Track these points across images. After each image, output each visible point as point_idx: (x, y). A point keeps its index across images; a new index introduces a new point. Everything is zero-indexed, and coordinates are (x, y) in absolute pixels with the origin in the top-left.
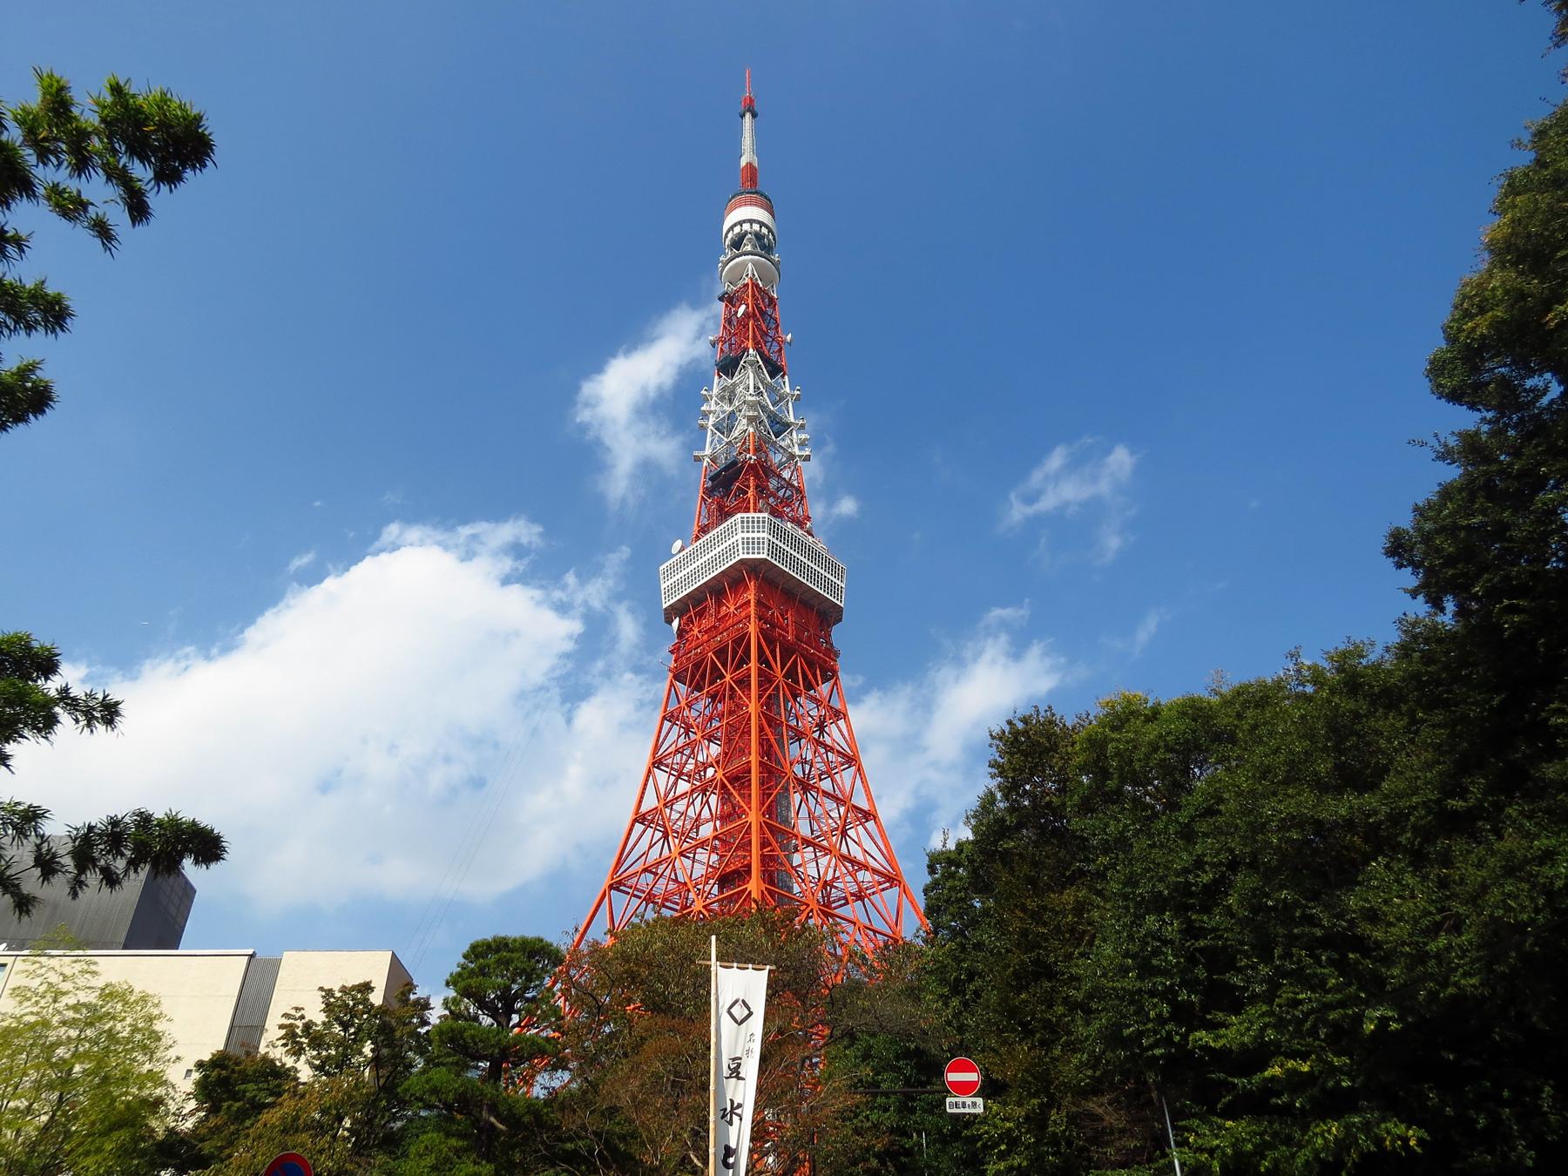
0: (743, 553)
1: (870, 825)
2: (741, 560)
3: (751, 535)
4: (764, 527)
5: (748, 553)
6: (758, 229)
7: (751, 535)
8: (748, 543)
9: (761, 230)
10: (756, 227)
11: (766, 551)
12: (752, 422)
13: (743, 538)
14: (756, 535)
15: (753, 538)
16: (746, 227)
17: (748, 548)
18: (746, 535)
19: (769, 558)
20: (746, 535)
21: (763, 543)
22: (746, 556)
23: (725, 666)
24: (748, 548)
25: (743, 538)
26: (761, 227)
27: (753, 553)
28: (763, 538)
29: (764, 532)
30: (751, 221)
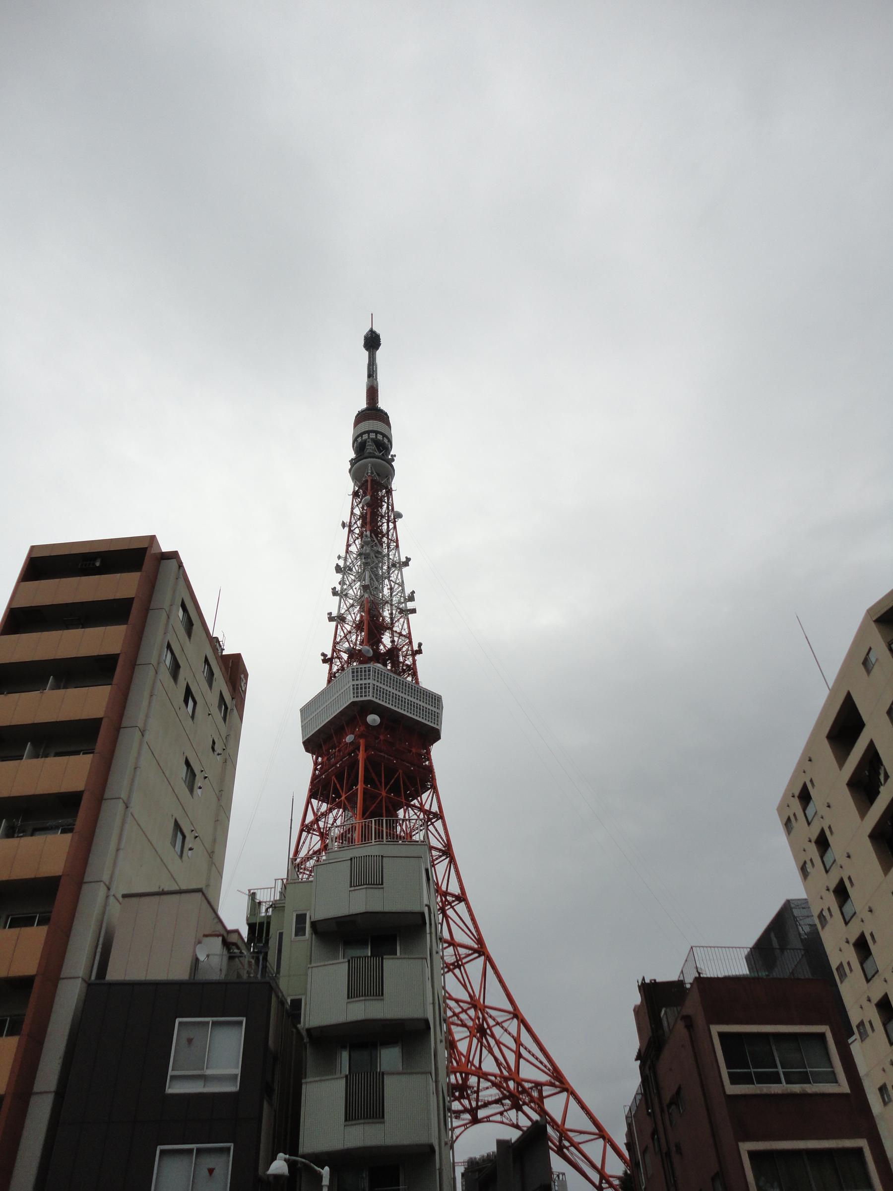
0: (354, 697)
1: (461, 907)
3: (359, 682)
5: (357, 697)
6: (374, 437)
7: (359, 682)
9: (376, 437)
10: (373, 436)
11: (371, 694)
13: (353, 685)
14: (363, 682)
15: (361, 684)
16: (365, 437)
18: (355, 682)
19: (374, 699)
20: (355, 682)
21: (369, 688)
22: (356, 699)
25: (353, 685)
26: (376, 435)
27: (361, 696)
28: (369, 684)
29: (369, 679)
30: (368, 432)
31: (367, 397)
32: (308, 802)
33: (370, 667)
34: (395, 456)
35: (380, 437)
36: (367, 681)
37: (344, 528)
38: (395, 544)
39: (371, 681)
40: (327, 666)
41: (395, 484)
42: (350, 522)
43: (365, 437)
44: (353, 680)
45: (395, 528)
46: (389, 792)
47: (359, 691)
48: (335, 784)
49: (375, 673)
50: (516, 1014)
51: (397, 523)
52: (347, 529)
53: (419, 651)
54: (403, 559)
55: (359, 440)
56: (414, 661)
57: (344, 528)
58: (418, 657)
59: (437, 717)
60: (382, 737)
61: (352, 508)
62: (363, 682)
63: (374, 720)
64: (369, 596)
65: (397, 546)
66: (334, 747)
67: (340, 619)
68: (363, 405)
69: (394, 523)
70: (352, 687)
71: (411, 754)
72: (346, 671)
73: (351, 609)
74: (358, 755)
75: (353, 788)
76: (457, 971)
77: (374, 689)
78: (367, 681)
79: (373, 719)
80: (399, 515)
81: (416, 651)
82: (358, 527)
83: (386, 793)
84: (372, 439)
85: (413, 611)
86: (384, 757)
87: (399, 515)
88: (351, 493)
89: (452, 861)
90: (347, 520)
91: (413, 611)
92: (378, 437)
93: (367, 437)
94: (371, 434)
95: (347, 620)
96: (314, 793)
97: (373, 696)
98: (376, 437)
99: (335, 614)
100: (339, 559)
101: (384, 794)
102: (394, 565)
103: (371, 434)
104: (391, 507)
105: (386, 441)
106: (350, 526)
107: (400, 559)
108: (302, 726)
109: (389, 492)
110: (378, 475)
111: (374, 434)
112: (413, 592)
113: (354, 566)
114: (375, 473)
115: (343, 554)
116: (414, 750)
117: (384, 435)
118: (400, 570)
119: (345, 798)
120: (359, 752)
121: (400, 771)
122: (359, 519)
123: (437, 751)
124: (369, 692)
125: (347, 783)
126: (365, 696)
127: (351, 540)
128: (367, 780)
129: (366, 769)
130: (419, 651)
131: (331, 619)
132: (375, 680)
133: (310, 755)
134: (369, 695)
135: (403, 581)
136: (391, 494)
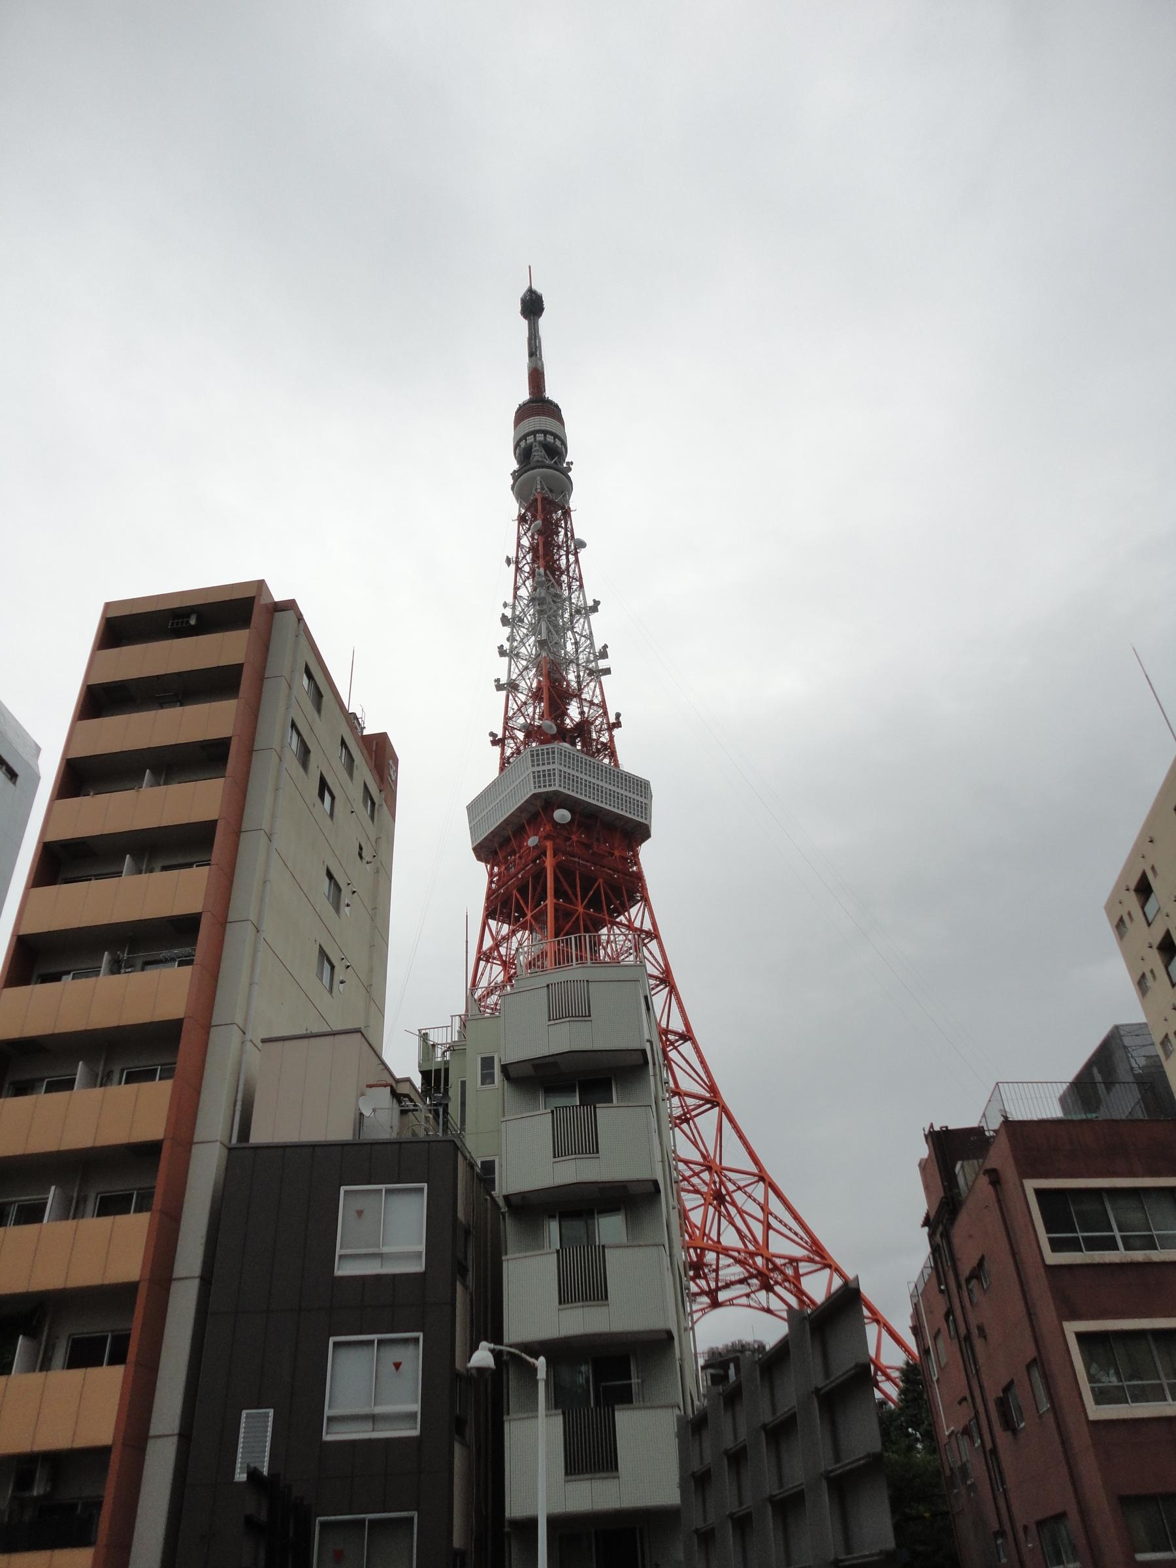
0: (535, 787)
1: (687, 1048)
2: (534, 795)
3: (541, 768)
4: (553, 758)
5: (540, 787)
6: (543, 438)
7: (541, 768)
8: (539, 777)
9: (545, 439)
10: (540, 437)
11: (557, 782)
12: (543, 647)
13: (534, 772)
14: (546, 767)
15: (544, 771)
16: (530, 439)
17: (539, 782)
18: (536, 769)
19: (561, 789)
20: (536, 769)
21: (554, 775)
23: (526, 903)
24: (539, 782)
25: (534, 772)
26: (545, 436)
27: (545, 786)
28: (554, 770)
29: (554, 763)
30: (534, 433)
31: (529, 384)
32: (485, 924)
33: (554, 748)
34: (572, 463)
35: (550, 439)
36: (551, 767)
37: (509, 566)
38: (578, 583)
39: (556, 766)
40: (498, 749)
41: (574, 502)
42: (517, 557)
43: (530, 439)
44: (533, 766)
45: (577, 561)
46: (587, 907)
47: (542, 779)
48: (517, 900)
49: (561, 755)
50: (762, 1177)
51: (579, 555)
52: (513, 566)
53: (618, 724)
54: (590, 603)
55: (523, 444)
56: (611, 737)
57: (509, 566)
58: (616, 732)
59: (645, 809)
60: (574, 838)
61: (519, 538)
62: (546, 767)
63: (563, 815)
64: (548, 655)
65: (581, 586)
66: (513, 853)
67: (512, 687)
68: (525, 396)
69: (576, 554)
70: (531, 775)
71: (614, 857)
72: (523, 755)
73: (525, 673)
74: (544, 862)
75: (541, 904)
76: (685, 1126)
77: (560, 776)
78: (551, 767)
79: (562, 815)
80: (581, 544)
81: (614, 724)
82: (528, 563)
83: (584, 908)
84: (540, 442)
85: (607, 671)
86: (579, 863)
87: (581, 544)
88: (516, 518)
89: (673, 990)
90: (513, 555)
91: (607, 671)
92: (548, 439)
93: (533, 440)
94: (537, 435)
95: (520, 688)
96: (491, 912)
97: (560, 786)
98: (545, 439)
99: (504, 680)
100: (505, 608)
101: (581, 909)
102: (578, 612)
103: (537, 435)
104: (569, 531)
105: (558, 443)
106: (517, 563)
107: (585, 602)
108: (471, 828)
109: (567, 513)
110: (551, 491)
111: (543, 435)
112: (605, 647)
113: (526, 616)
114: (546, 489)
115: (510, 600)
116: (617, 853)
117: (556, 436)
118: (587, 617)
119: (532, 916)
120: (546, 858)
121: (601, 880)
122: (528, 553)
123: (647, 853)
124: (554, 780)
125: (533, 898)
126: (550, 785)
127: (520, 581)
128: (557, 895)
129: (556, 880)
130: (618, 724)
131: (499, 687)
132: (561, 764)
133: (483, 864)
134: (555, 785)
135: (591, 633)
136: (570, 516)
